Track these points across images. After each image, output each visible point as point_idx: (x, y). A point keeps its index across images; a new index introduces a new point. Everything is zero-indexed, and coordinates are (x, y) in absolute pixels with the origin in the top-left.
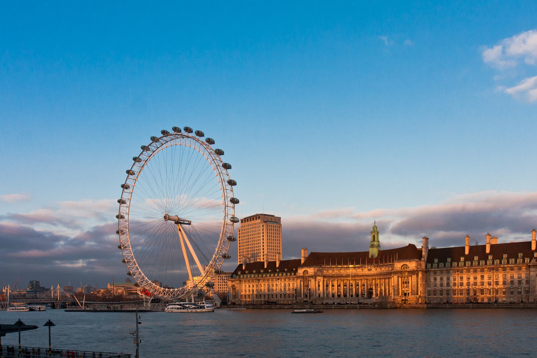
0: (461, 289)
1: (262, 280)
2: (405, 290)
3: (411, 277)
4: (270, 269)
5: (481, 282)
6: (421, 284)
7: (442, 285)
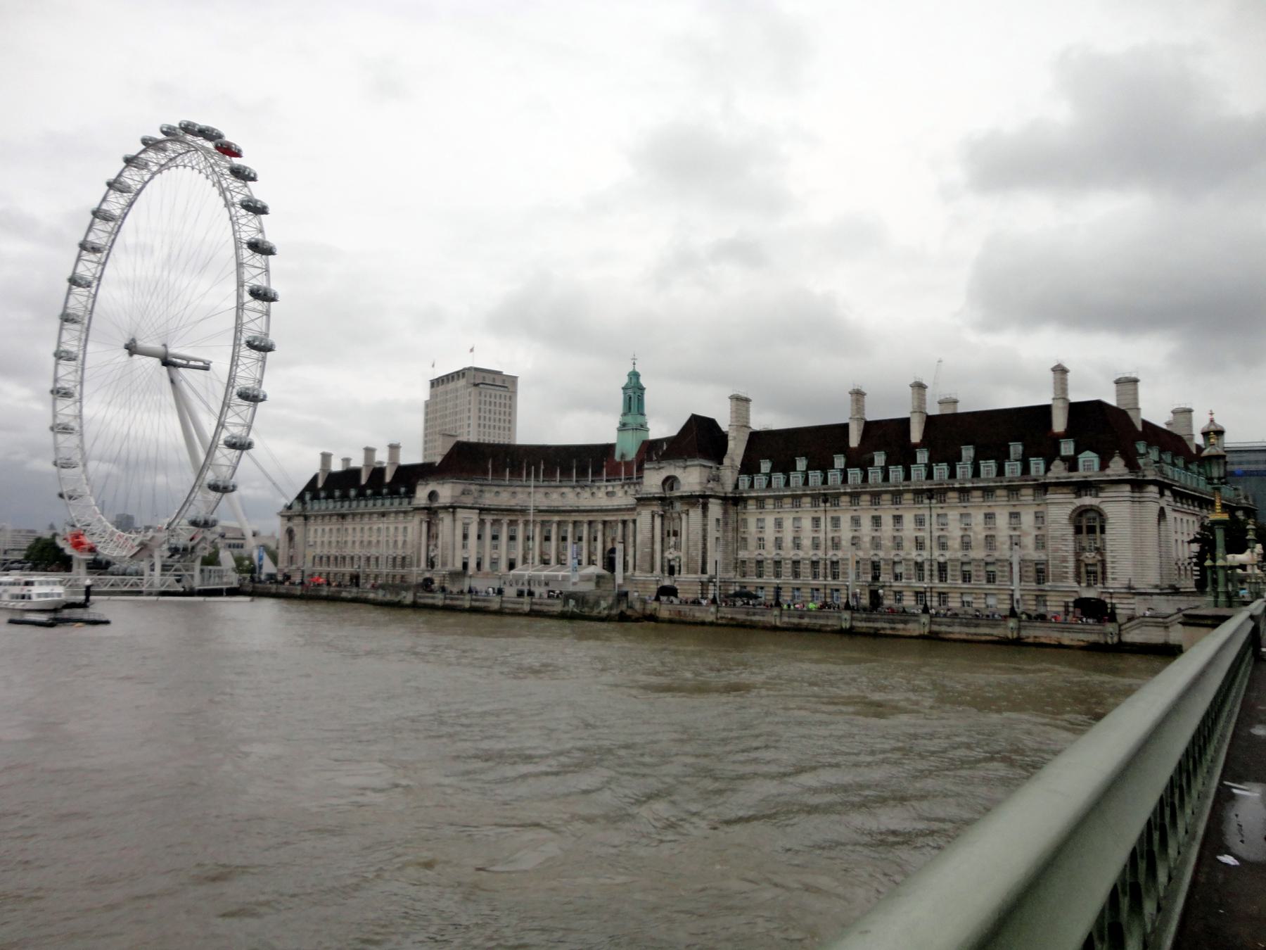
0: (835, 559)
1: (351, 516)
2: (671, 557)
3: (688, 514)
4: (371, 488)
5: (894, 537)
6: (717, 538)
7: (778, 544)
